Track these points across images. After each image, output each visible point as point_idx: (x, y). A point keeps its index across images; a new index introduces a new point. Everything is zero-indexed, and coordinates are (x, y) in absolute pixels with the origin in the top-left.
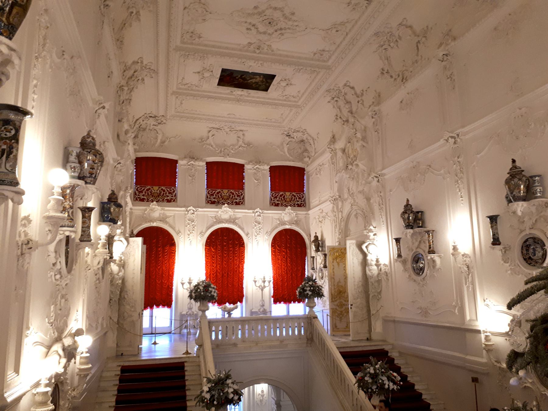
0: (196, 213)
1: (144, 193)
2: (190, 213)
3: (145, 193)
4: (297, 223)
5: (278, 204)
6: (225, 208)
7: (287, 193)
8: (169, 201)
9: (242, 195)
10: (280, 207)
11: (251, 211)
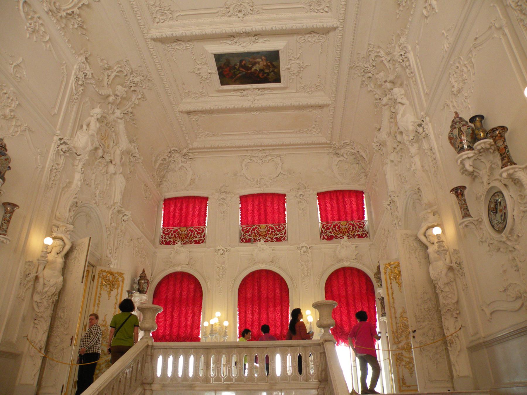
0: (226, 253)
1: (170, 235)
2: (219, 254)
3: (172, 235)
6: (261, 244)
7: (342, 222)
10: (334, 240)
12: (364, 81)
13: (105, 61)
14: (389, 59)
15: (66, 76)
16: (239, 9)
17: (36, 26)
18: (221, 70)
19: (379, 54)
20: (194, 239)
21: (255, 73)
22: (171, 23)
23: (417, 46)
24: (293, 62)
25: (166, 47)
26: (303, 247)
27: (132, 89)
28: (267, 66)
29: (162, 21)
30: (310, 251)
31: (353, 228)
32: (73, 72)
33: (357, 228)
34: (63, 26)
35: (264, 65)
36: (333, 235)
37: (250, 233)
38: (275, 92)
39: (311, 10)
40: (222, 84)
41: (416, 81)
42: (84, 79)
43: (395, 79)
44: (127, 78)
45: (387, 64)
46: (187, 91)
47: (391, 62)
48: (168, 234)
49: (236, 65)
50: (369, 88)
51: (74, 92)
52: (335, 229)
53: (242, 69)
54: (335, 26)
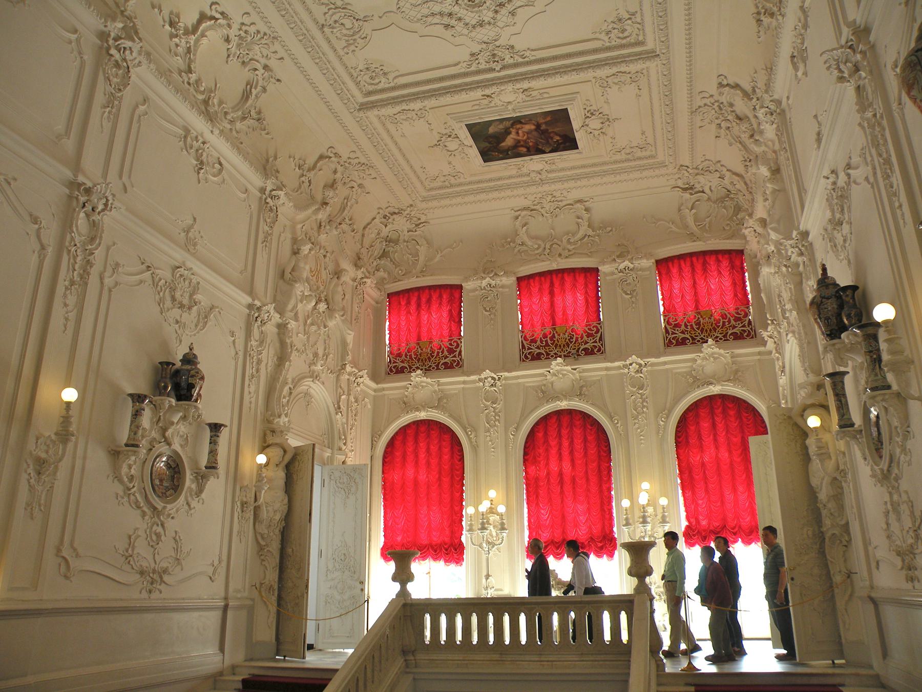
0: (498, 383)
2: (487, 384)
3: (406, 355)
4: (735, 376)
5: (684, 339)
6: (557, 364)
8: (448, 366)
9: (597, 332)
11: (617, 364)
20: (442, 362)
26: (631, 364)
30: (645, 369)
31: (724, 323)
33: (733, 322)
36: (688, 336)
37: (539, 342)
48: (399, 355)
52: (691, 326)
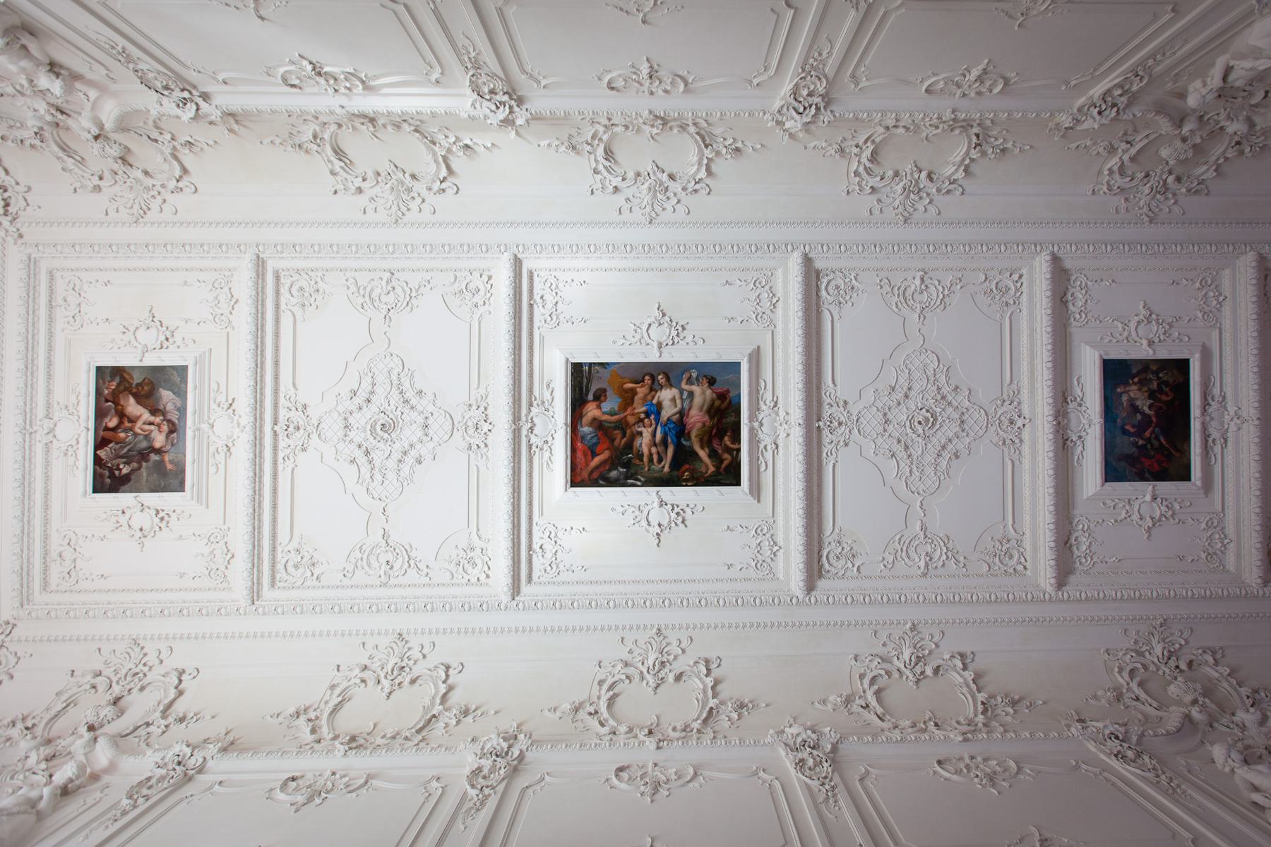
12: (1189, 191)
13: (1100, 693)
14: (1124, 146)
15: (1106, 774)
16: (1006, 422)
17: (982, 770)
18: (1147, 475)
19: (1116, 168)
21: (1160, 408)
22: (1027, 544)
23: (1073, 83)
24: (1133, 333)
25: (1081, 568)
27: (1183, 666)
28: (1142, 383)
29: (1022, 560)
32: (1103, 757)
34: (1002, 729)
35: (1140, 390)
38: (1216, 372)
39: (1017, 302)
40: (1185, 476)
41: (1152, 56)
42: (1126, 745)
43: (1168, 115)
44: (1152, 668)
45: (1138, 147)
46: (1203, 556)
47: (1130, 139)
49: (1135, 444)
50: (1211, 174)
51: (1150, 775)
53: (1147, 434)
54: (1048, 258)
